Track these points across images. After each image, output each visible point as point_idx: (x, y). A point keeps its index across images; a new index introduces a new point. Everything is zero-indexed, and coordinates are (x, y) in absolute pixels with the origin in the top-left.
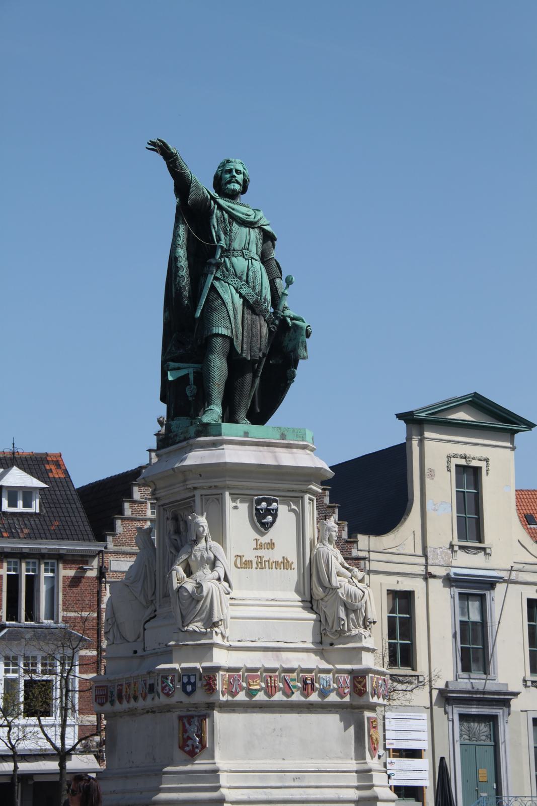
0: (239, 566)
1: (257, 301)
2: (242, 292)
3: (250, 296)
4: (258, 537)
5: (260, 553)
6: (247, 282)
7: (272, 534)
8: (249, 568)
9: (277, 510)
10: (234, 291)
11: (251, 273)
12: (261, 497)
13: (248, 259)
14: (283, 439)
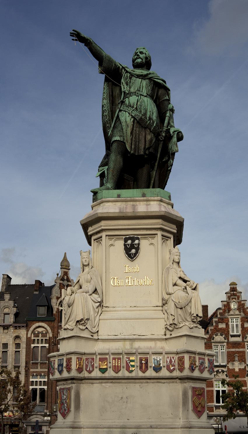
1: (141, 118)
2: (133, 115)
3: (137, 116)
6: (136, 108)
10: (127, 114)
11: (139, 103)
13: (139, 96)
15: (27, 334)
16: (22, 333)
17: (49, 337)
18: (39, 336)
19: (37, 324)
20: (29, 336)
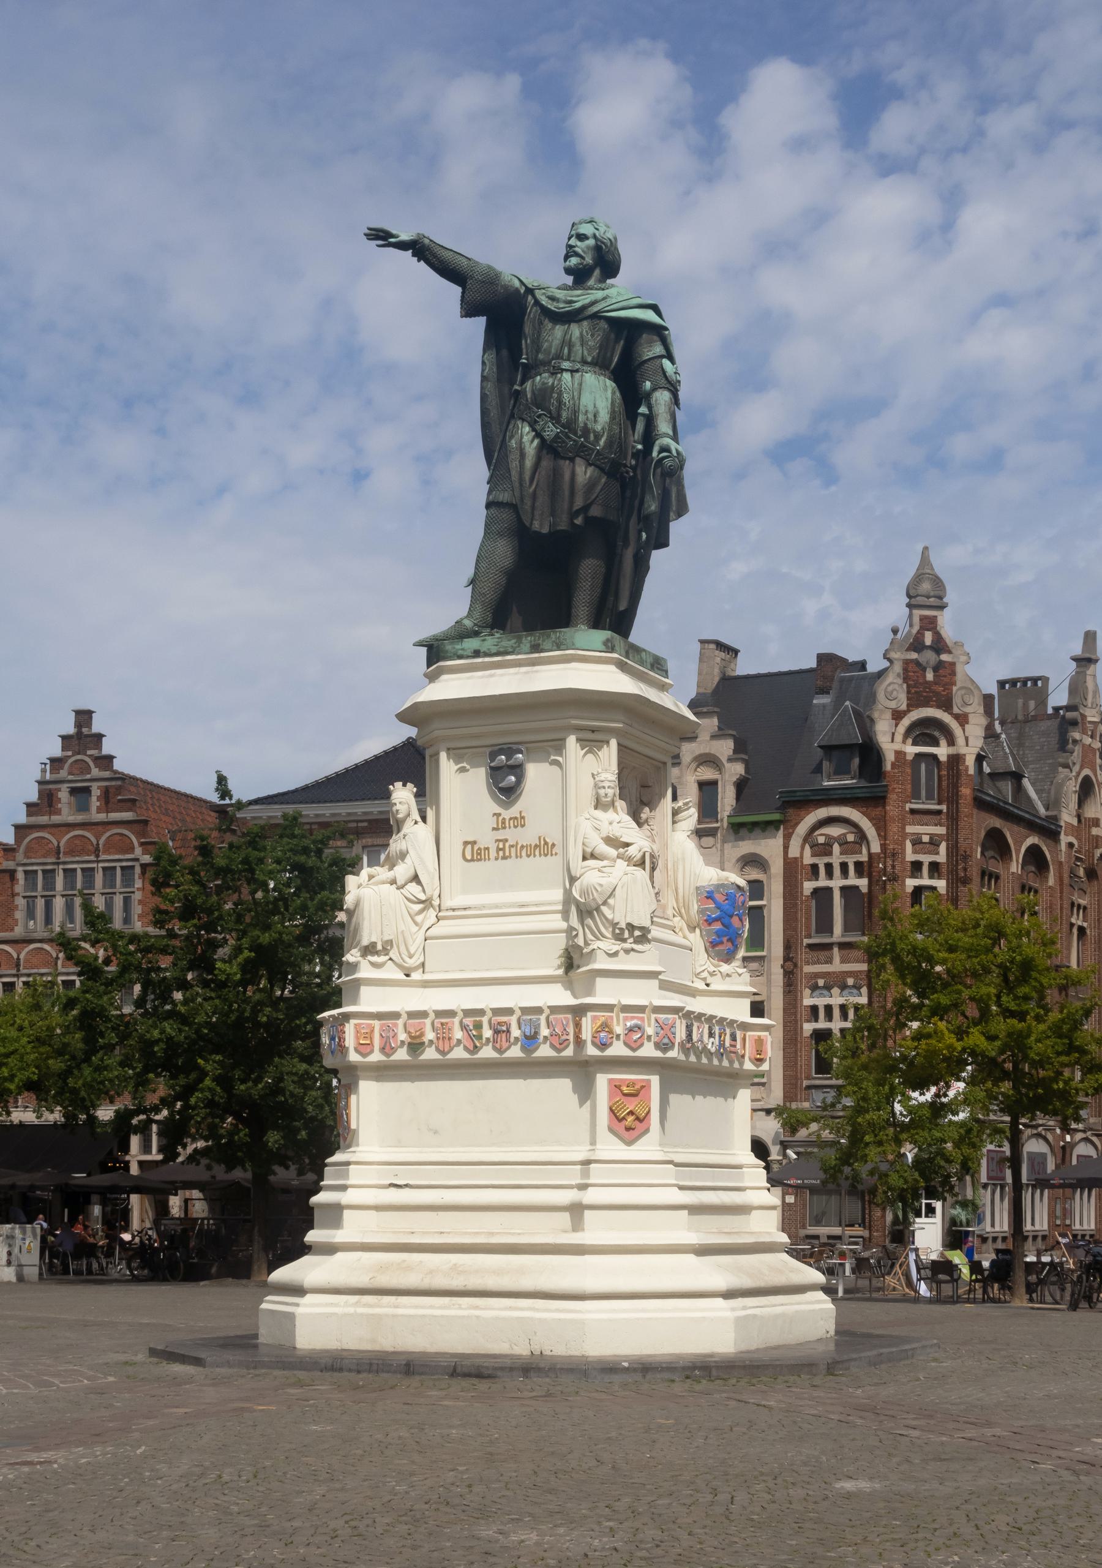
0: (469, 857)
1: (557, 436)
4: (498, 810)
5: (501, 835)
7: (524, 803)
15: (786, 848)
16: (771, 847)
17: (870, 855)
18: (830, 854)
19: (823, 813)
20: (794, 852)
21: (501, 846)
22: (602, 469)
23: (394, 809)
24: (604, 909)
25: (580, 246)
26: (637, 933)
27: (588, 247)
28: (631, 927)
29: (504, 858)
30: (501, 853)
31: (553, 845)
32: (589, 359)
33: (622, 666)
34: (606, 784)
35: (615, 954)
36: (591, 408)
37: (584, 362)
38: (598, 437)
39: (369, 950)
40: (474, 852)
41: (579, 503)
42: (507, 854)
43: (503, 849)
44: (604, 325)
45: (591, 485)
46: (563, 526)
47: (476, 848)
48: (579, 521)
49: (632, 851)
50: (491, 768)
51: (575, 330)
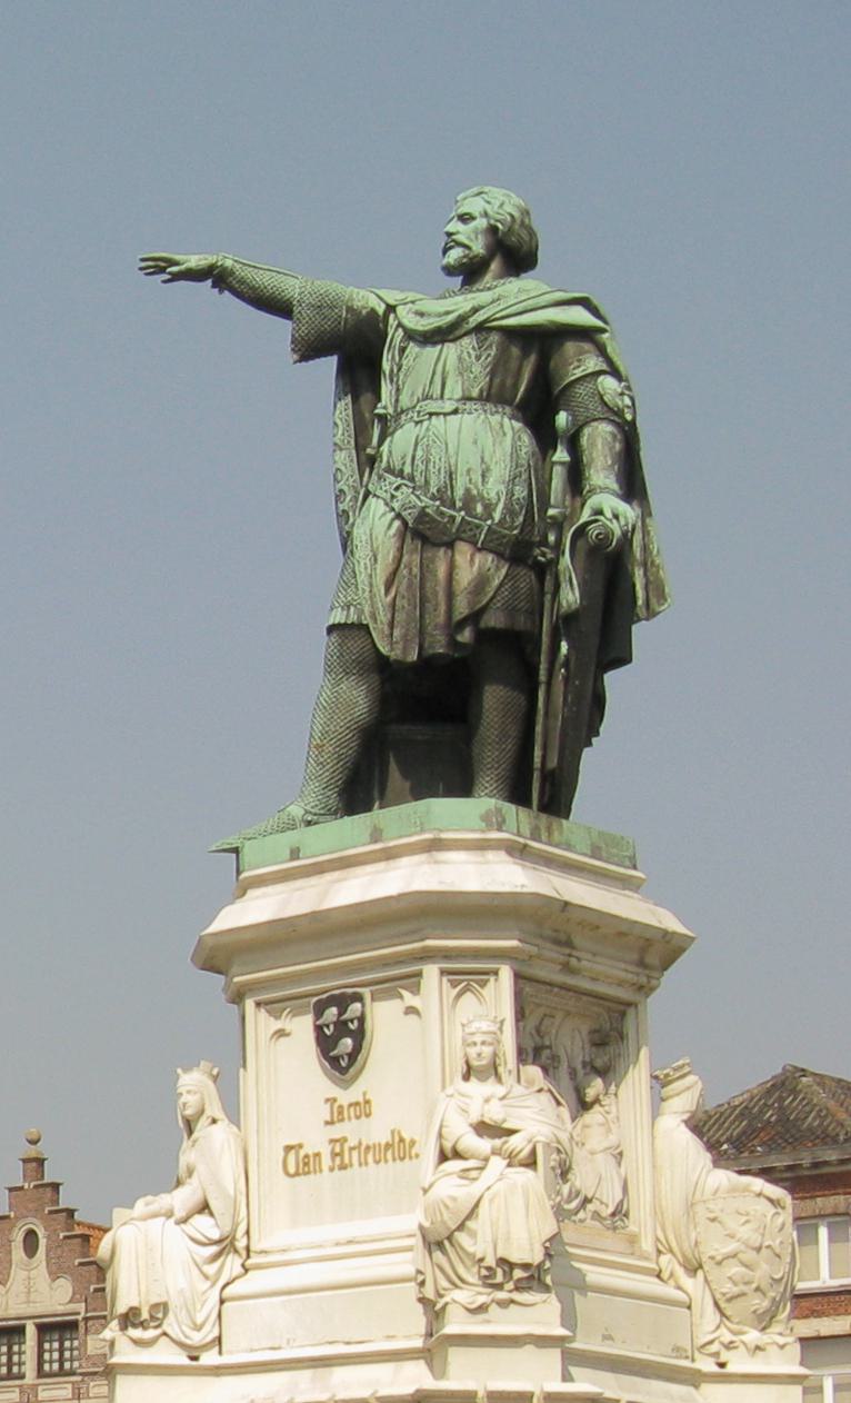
0: (292, 1170)
4: (335, 1091)
5: (338, 1131)
8: (315, 1172)
9: (362, 1019)
10: (382, 508)
11: (419, 453)
12: (324, 996)
14: (376, 842)
21: (337, 1150)
22: (500, 555)
23: (182, 1100)
24: (461, 1237)
25: (463, 232)
26: (518, 1274)
27: (476, 232)
28: (502, 1261)
29: (343, 1167)
30: (338, 1160)
31: (413, 1143)
32: (475, 393)
33: (519, 852)
34: (478, 1038)
35: (482, 1309)
36: (475, 463)
37: (466, 398)
38: (489, 508)
39: (130, 1319)
40: (302, 1164)
41: (462, 608)
42: (346, 1161)
43: (340, 1154)
44: (495, 338)
45: (481, 583)
46: (439, 646)
47: (302, 1153)
48: (466, 636)
49: (514, 1142)
50: (319, 1029)
51: (451, 351)
